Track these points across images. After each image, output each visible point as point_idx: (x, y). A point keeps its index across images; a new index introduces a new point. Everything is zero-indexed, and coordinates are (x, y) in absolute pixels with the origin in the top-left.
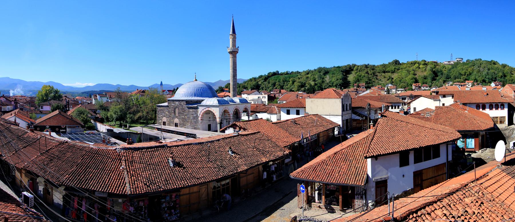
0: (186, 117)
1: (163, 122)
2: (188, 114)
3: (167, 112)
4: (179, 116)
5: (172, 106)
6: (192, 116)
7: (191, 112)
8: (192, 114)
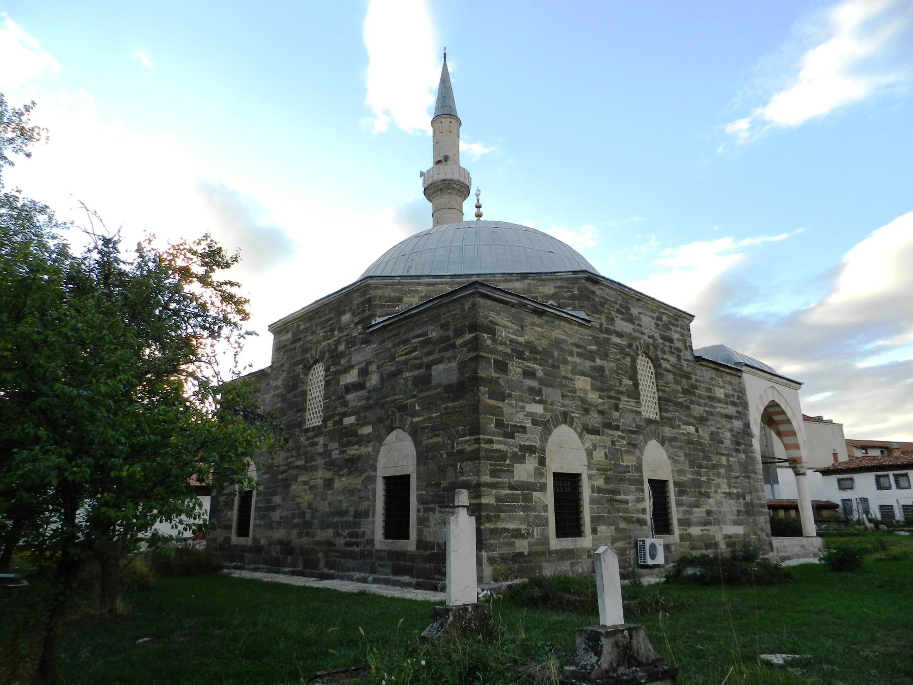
0: (704, 433)
1: (556, 476)
3: (582, 383)
4: (670, 422)
5: (620, 335)
7: (719, 401)
8: (728, 417)
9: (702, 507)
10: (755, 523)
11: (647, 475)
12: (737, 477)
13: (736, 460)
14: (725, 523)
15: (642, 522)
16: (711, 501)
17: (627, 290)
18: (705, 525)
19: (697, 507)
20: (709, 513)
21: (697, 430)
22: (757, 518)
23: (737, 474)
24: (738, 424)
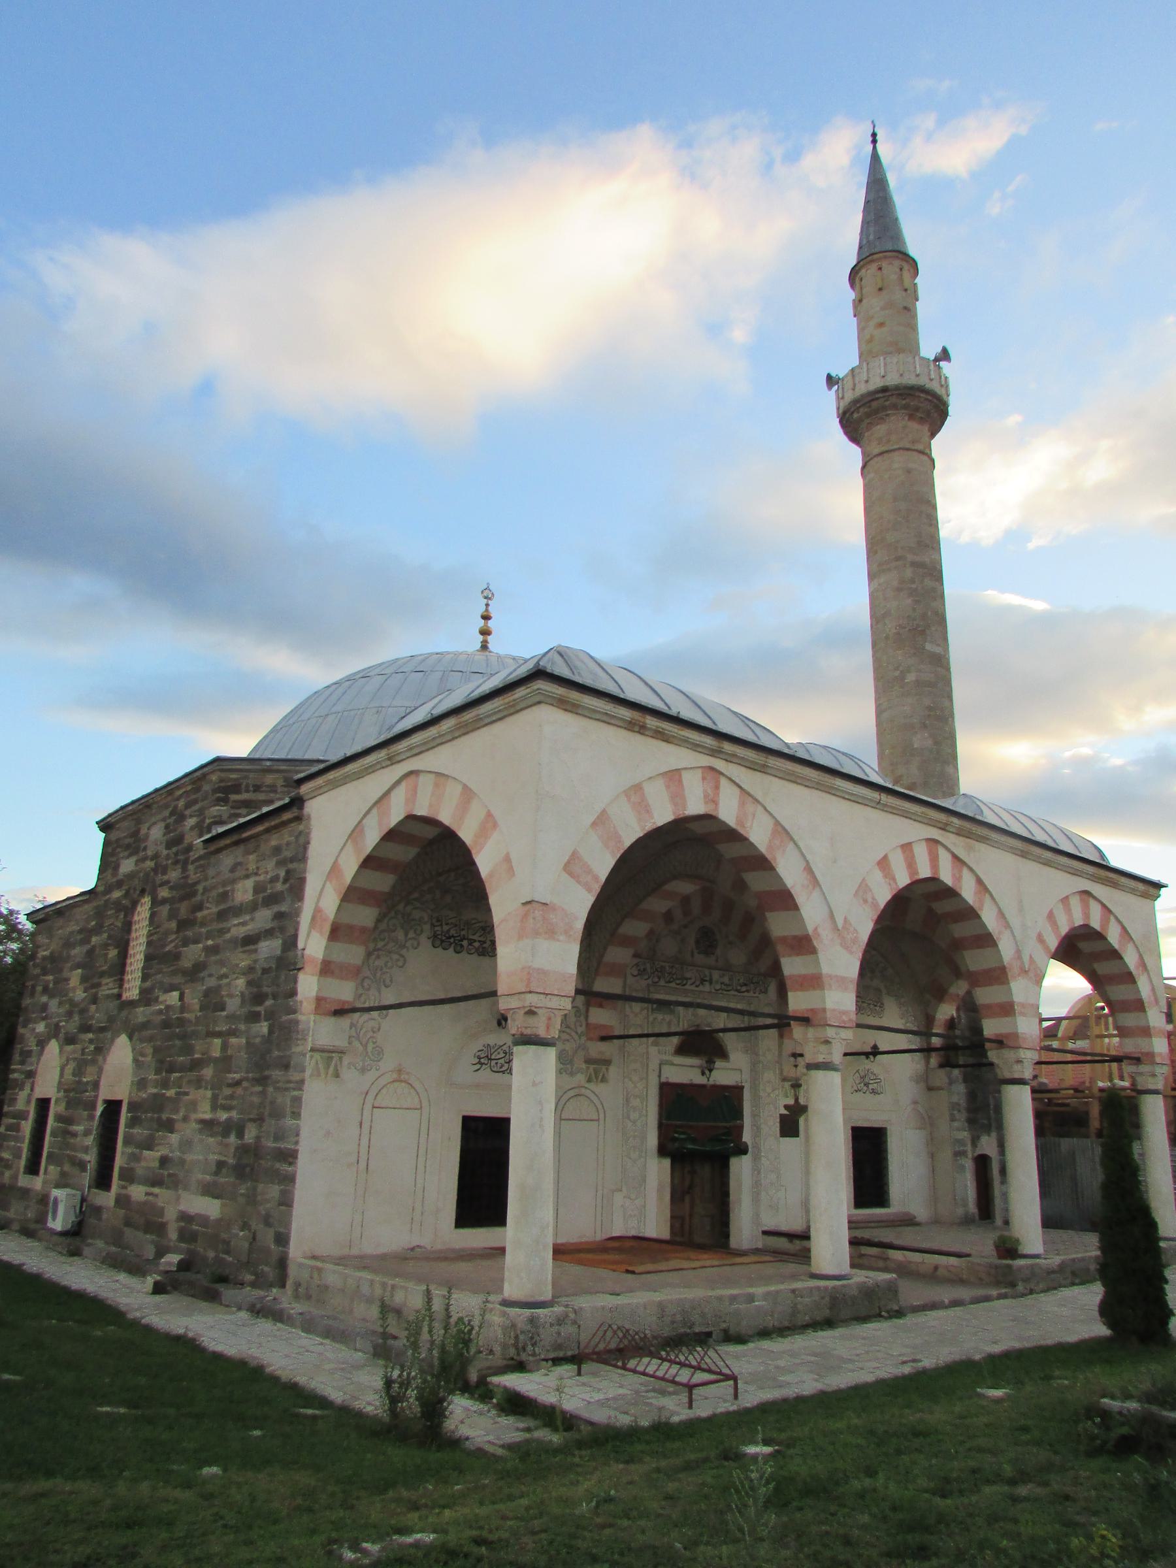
2: (214, 950)
6: (251, 969)
9: (156, 1149)
10: (252, 1199)
11: (106, 1093)
12: (238, 1083)
13: (244, 1041)
14: (185, 1188)
15: (82, 1166)
16: (174, 1138)
17: (130, 808)
18: (153, 1185)
19: (150, 1148)
20: (164, 1161)
21: (181, 998)
22: (261, 1187)
23: (237, 1076)
24: (269, 948)
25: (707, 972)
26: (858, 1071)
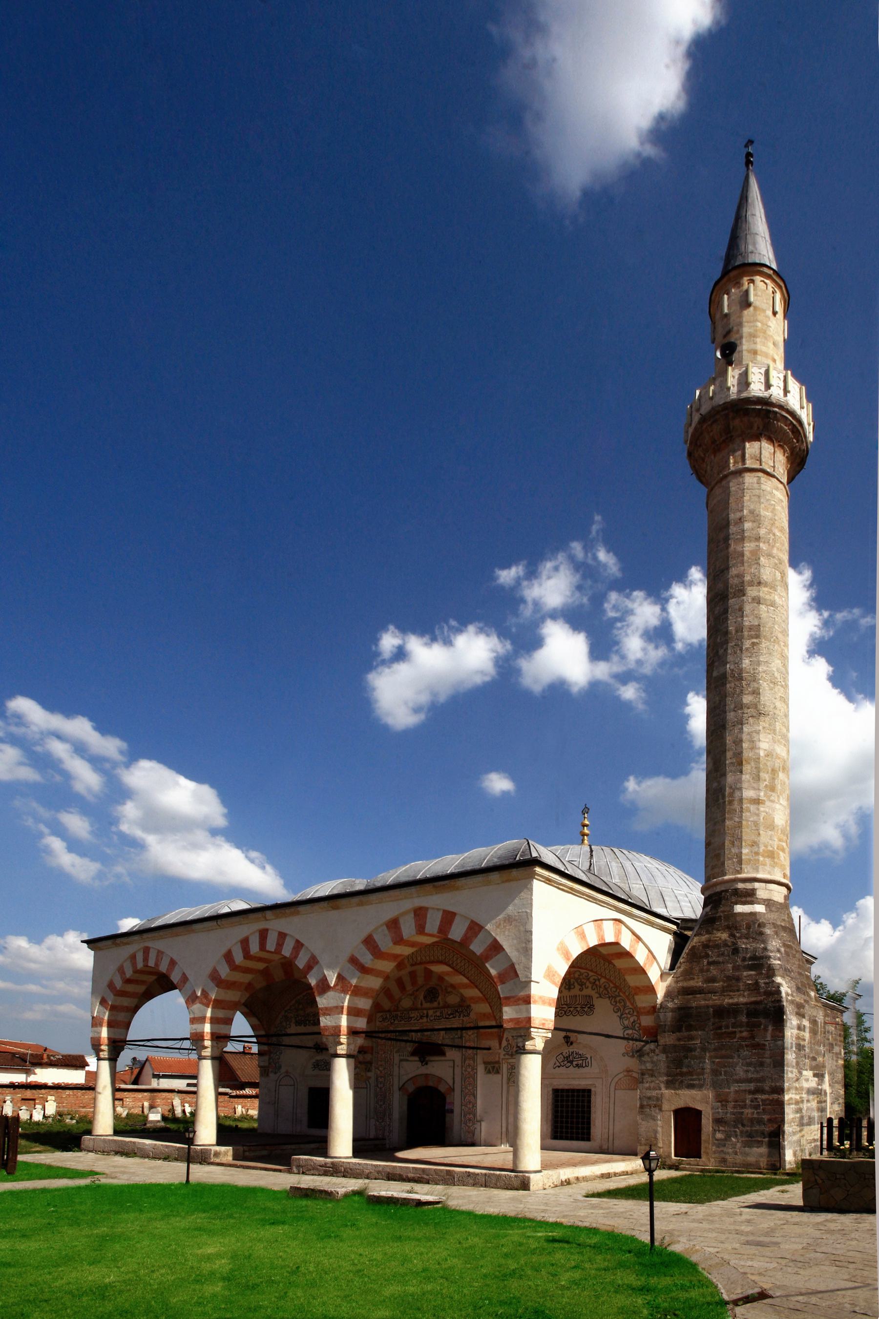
25: (425, 1012)
26: (562, 1054)
